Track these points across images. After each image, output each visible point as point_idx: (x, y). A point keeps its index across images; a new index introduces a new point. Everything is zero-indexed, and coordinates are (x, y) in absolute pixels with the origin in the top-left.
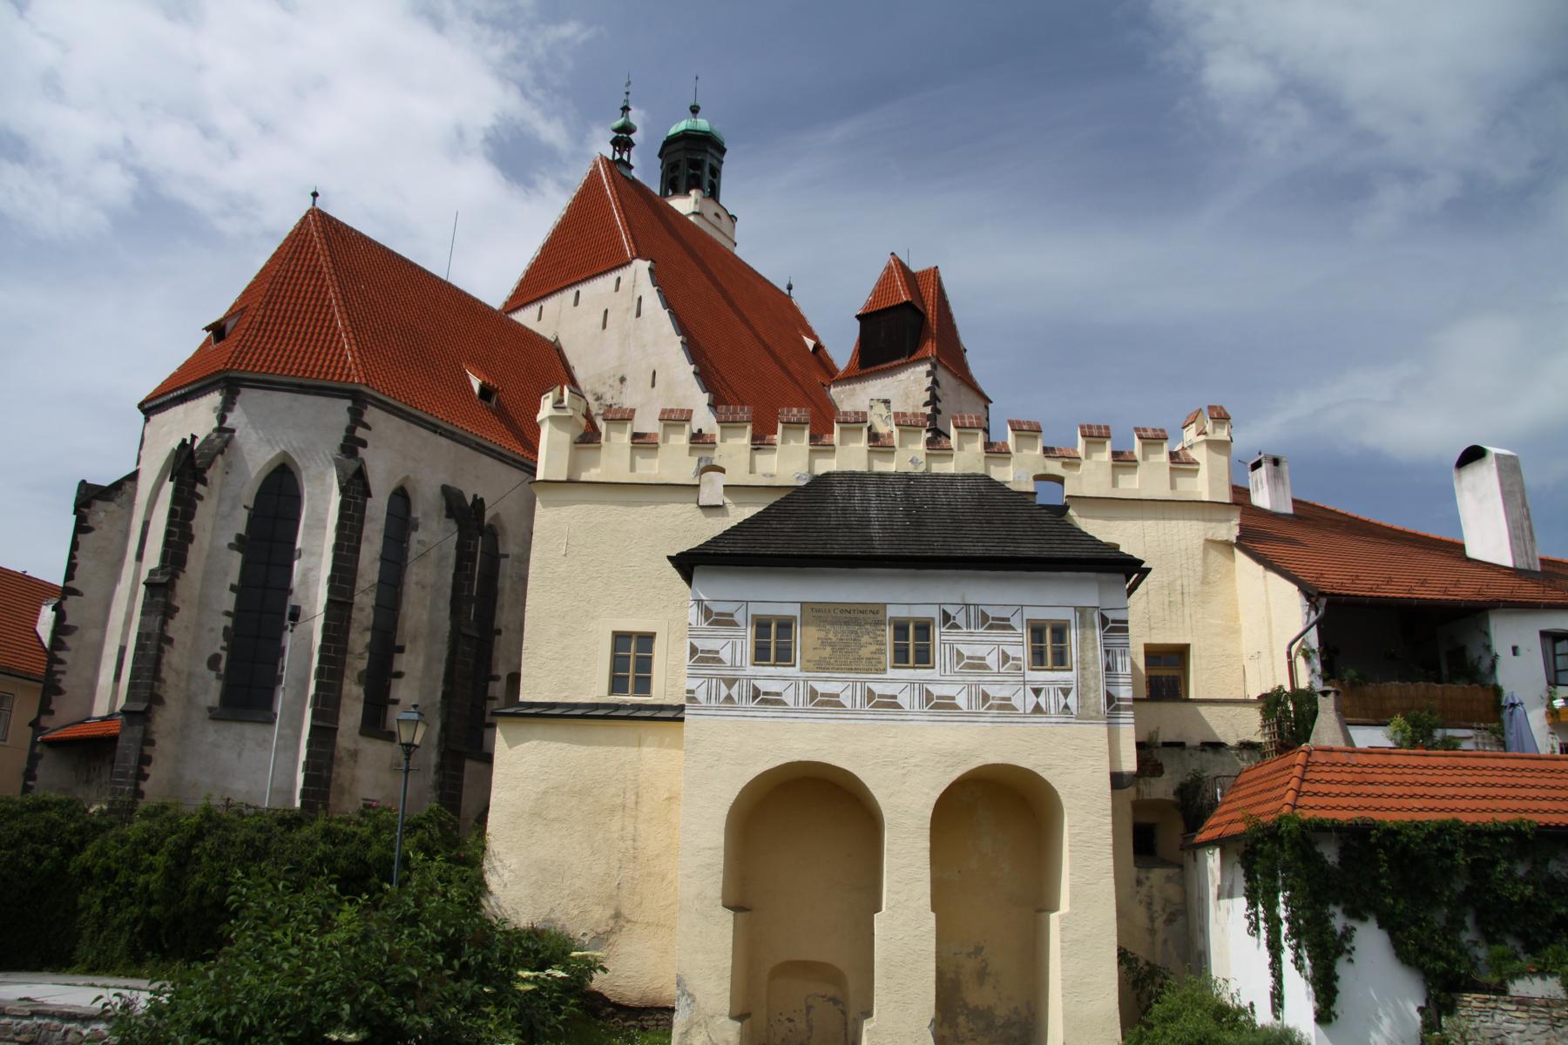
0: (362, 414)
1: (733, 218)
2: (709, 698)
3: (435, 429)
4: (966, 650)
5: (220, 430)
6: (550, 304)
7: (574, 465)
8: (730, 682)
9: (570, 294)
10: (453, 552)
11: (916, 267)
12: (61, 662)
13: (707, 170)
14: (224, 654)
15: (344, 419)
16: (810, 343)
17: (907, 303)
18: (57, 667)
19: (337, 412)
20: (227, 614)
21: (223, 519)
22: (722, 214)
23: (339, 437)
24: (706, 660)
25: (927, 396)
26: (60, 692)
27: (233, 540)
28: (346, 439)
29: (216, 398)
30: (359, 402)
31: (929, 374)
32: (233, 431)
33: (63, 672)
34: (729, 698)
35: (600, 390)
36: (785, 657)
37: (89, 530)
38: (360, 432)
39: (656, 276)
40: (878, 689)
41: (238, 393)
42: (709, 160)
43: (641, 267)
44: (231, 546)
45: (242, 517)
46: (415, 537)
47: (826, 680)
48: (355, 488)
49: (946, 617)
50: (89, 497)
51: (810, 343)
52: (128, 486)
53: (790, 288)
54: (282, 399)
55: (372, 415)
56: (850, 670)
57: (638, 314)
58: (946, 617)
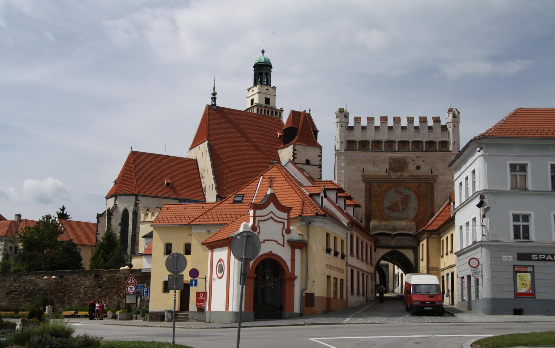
1: (274, 88)
3: (153, 197)
5: (115, 204)
7: (145, 218)
13: (264, 75)
15: (134, 200)
16: (279, 135)
19: (133, 198)
23: (134, 204)
25: (292, 154)
29: (114, 198)
30: (137, 196)
31: (293, 148)
38: (137, 202)
43: (207, 142)
45: (120, 219)
50: (99, 216)
51: (279, 135)
54: (124, 197)
55: (139, 198)
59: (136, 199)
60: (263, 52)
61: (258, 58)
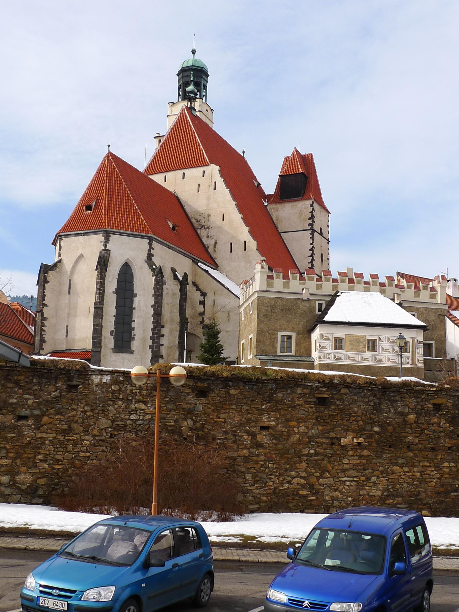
0: (152, 245)
2: (324, 358)
4: (385, 348)
6: (170, 175)
8: (329, 354)
9: (180, 172)
10: (179, 293)
11: (302, 153)
12: (44, 331)
14: (114, 330)
15: (147, 247)
17: (302, 173)
18: (43, 333)
20: (115, 316)
21: (111, 285)
22: (209, 110)
24: (323, 348)
25: (310, 215)
26: (45, 341)
27: (114, 291)
28: (148, 254)
29: (101, 237)
30: (151, 240)
31: (311, 206)
32: (110, 251)
33: (45, 335)
34: (329, 358)
35: (199, 218)
36: (341, 348)
37: (48, 282)
38: (152, 252)
39: (223, 173)
40: (364, 356)
41: (110, 236)
42: (203, 82)
43: (215, 169)
44: (113, 292)
45: (116, 281)
46: (165, 287)
47: (352, 354)
48: (158, 273)
49: (380, 339)
52: (58, 265)
53: (244, 152)
55: (155, 245)
56: (357, 352)
57: (215, 189)
58: (380, 339)
59: (150, 244)
60: (194, 52)
61: (185, 59)
